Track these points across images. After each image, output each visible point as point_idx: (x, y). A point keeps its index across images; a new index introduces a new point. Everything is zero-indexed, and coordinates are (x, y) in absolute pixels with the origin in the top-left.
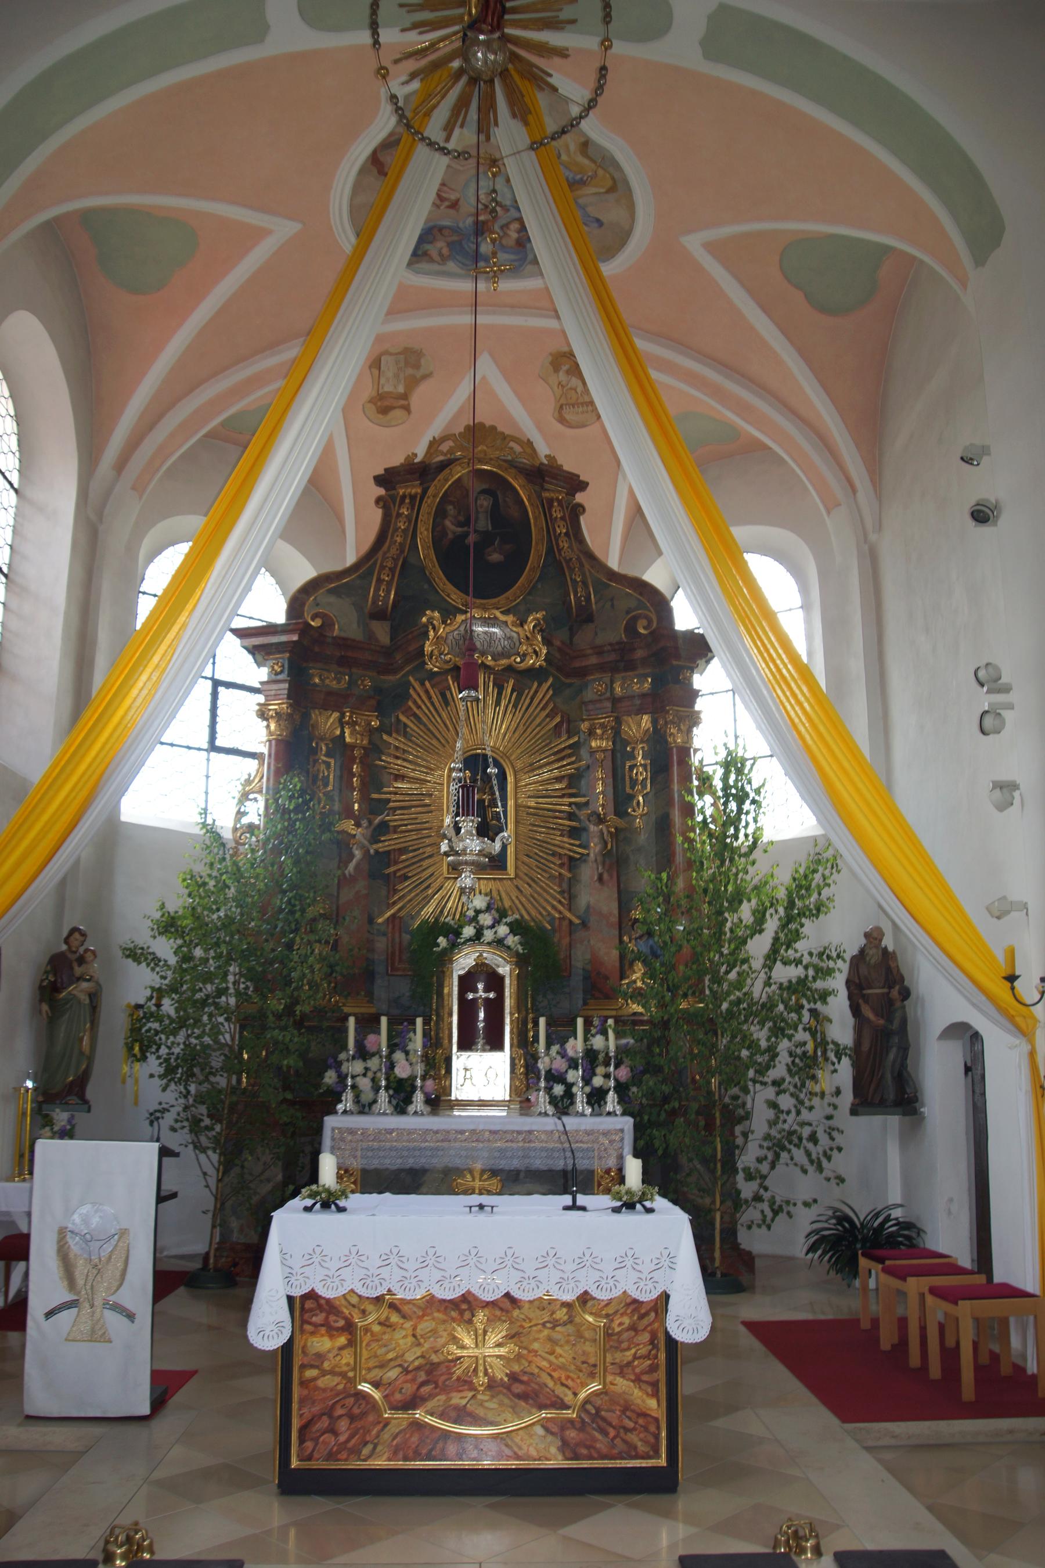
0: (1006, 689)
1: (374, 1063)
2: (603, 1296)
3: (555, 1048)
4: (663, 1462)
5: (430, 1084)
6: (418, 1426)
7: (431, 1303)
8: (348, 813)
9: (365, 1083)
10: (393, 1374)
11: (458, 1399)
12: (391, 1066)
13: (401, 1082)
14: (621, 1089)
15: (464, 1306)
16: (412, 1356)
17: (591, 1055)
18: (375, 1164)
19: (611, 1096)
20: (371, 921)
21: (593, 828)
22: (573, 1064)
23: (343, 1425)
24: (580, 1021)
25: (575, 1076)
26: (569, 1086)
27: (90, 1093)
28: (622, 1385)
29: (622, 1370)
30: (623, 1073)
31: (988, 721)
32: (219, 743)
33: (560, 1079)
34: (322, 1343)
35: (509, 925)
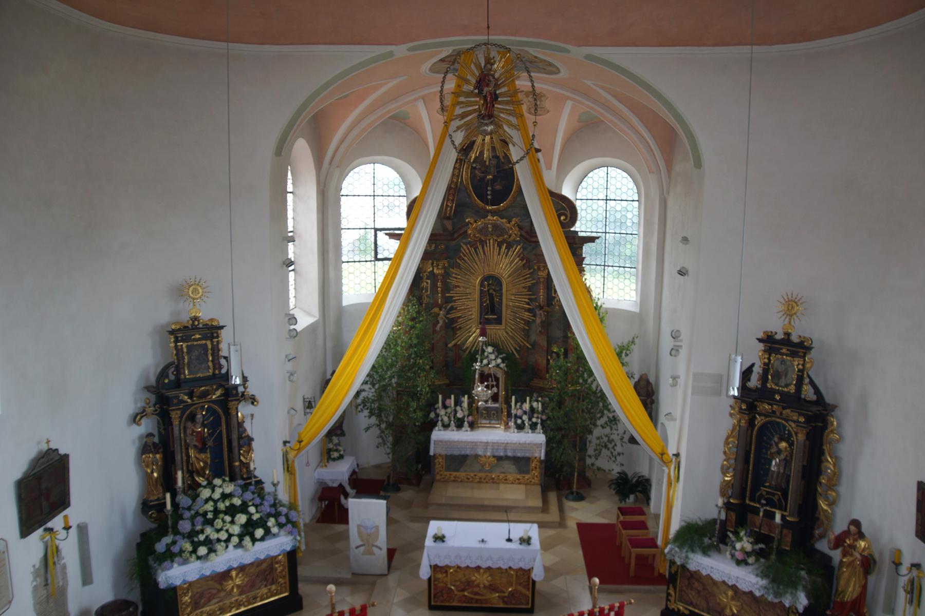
0: (681, 341)
1: (449, 410)
2: (515, 567)
3: (519, 404)
4: (529, 606)
5: (470, 418)
6: (464, 596)
7: (468, 567)
8: (436, 305)
9: (446, 419)
10: (458, 583)
11: (476, 590)
12: (456, 412)
13: (459, 419)
14: (543, 422)
15: (478, 568)
16: (463, 579)
17: (532, 410)
18: (449, 453)
19: (539, 426)
20: (446, 345)
21: (538, 312)
22: (525, 413)
23: (445, 595)
24: (528, 399)
25: (525, 417)
26: (523, 422)
27: (345, 427)
28: (519, 588)
29: (520, 584)
30: (544, 417)
31: (673, 352)
32: (379, 256)
33: (521, 418)
34: (439, 576)
35: (502, 359)
